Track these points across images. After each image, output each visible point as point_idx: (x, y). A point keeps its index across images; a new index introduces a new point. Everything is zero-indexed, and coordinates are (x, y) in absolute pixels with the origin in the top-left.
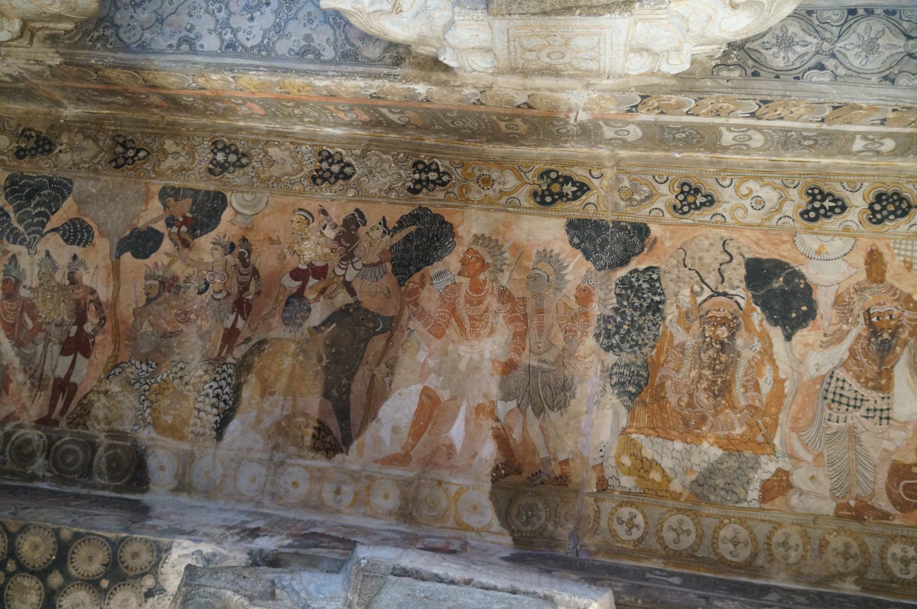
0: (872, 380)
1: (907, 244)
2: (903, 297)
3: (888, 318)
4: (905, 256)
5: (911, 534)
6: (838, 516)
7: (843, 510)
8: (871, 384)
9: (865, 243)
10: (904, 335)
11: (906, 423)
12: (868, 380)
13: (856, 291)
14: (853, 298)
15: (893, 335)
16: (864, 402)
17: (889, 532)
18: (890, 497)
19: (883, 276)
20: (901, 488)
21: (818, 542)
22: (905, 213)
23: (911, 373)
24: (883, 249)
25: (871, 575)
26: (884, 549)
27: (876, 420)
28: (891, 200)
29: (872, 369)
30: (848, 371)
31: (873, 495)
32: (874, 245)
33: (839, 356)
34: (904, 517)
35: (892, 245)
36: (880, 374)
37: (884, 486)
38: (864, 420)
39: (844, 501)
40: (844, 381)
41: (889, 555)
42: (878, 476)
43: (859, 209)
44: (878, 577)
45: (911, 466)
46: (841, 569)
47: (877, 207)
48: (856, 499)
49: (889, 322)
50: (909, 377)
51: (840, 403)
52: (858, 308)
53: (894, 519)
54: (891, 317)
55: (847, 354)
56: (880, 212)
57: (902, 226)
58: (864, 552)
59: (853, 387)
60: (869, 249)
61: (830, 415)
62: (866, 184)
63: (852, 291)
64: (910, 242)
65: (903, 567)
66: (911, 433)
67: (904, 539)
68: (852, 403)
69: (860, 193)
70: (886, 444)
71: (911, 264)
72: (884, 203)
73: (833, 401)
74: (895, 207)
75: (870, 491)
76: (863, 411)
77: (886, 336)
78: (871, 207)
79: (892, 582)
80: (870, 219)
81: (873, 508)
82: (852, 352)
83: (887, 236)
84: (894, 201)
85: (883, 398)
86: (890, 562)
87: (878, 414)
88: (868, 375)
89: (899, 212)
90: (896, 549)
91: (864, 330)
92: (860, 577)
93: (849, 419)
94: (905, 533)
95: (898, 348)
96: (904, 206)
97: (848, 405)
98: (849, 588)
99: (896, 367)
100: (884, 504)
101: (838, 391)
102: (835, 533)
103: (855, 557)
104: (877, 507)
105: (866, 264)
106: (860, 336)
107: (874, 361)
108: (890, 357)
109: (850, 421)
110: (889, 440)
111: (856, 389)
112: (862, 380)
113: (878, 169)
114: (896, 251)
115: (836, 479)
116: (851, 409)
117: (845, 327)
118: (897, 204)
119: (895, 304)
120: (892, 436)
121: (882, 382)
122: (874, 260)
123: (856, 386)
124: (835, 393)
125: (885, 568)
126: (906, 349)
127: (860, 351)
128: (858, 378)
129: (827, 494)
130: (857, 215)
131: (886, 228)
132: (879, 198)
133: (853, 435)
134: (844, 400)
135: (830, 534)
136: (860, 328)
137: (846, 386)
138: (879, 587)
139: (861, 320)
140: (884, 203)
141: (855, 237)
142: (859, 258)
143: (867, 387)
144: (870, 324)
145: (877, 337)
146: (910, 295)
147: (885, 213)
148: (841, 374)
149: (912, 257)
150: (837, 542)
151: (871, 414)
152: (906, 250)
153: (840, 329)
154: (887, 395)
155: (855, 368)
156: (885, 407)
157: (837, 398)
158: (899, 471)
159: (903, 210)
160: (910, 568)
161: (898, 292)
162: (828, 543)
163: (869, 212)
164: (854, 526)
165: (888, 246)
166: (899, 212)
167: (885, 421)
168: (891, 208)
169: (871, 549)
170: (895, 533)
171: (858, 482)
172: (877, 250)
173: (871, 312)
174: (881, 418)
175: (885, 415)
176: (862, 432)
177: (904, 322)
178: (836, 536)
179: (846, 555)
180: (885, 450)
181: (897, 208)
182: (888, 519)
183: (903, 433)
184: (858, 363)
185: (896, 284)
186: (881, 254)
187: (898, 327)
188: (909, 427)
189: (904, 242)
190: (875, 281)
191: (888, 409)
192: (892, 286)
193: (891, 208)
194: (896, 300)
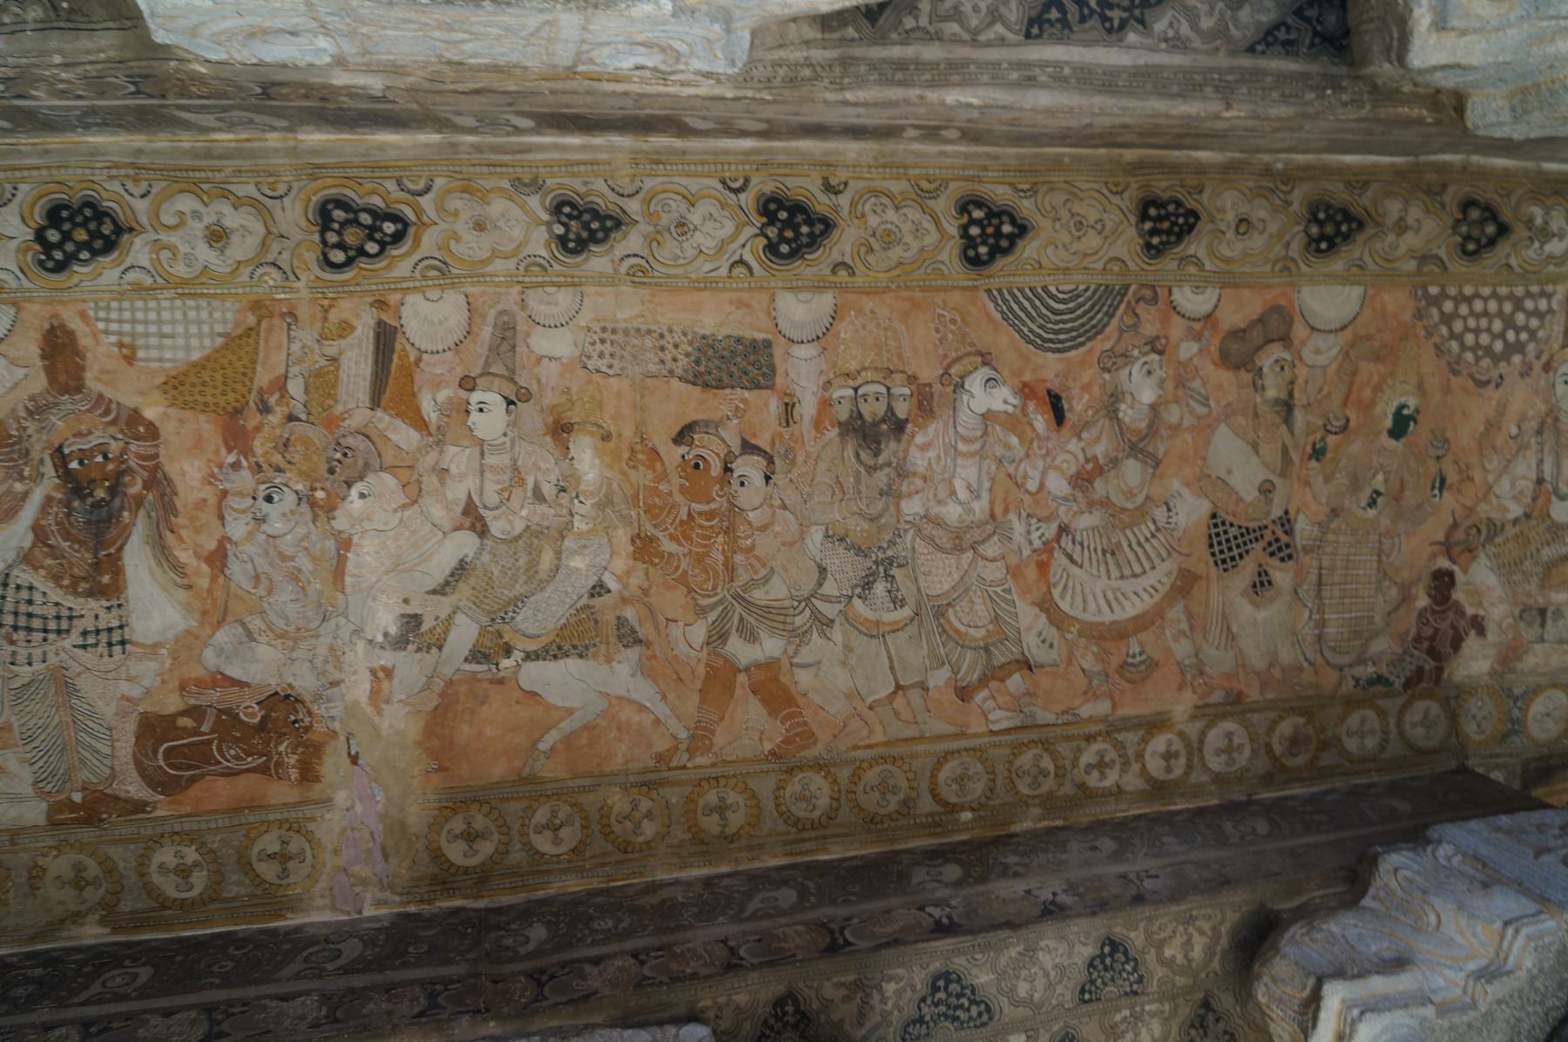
0: (84, 579)
1: (121, 309)
2: (124, 416)
3: (99, 459)
4: (120, 333)
5: (187, 827)
6: (54, 824)
7: (61, 812)
8: (83, 586)
9: (37, 315)
10: (135, 488)
11: (156, 646)
12: (76, 581)
13: (30, 413)
14: (25, 429)
15: (113, 491)
16: (75, 622)
17: (150, 832)
18: (143, 776)
19: (80, 379)
20: (160, 756)
21: (25, 873)
22: (110, 246)
23: (155, 556)
24: (75, 324)
25: (126, 906)
26: (143, 860)
27: (102, 648)
28: (79, 219)
29: (81, 558)
30: (36, 568)
31: (113, 776)
32: (56, 316)
33: (14, 543)
34: (171, 802)
35: (91, 313)
36: (97, 566)
37: (130, 758)
38: (80, 652)
39: (62, 797)
40: (31, 588)
41: (154, 867)
42: (117, 744)
43: (14, 243)
44: (139, 906)
45: (174, 717)
46: (73, 907)
47: (53, 236)
48: (84, 789)
49: (103, 465)
50: (153, 563)
51: (29, 629)
52: (38, 448)
53: (155, 808)
54: (105, 457)
55: (30, 537)
56: (59, 246)
57: (105, 273)
58: (110, 870)
59: (50, 595)
60: (47, 326)
61: (14, 653)
62: (24, 187)
63: (23, 414)
64: (126, 304)
65: (180, 880)
66: (168, 661)
67: (177, 838)
68: (52, 625)
69: (14, 207)
70: (124, 688)
71: (133, 348)
72: (66, 227)
73: (15, 628)
74: (89, 232)
75: (107, 771)
76: (74, 637)
77: (100, 493)
78: (40, 236)
79: (165, 908)
80: (41, 264)
81: (117, 798)
82: (38, 531)
83: (79, 296)
84: (87, 220)
85: (108, 608)
86: (156, 878)
87: (104, 637)
88: (76, 571)
89: (98, 244)
90: (165, 856)
91: (56, 488)
92: (109, 914)
93: (50, 655)
94: (177, 828)
95: (126, 514)
96: (107, 229)
97: (45, 631)
98: (92, 933)
99: (127, 548)
100: (134, 788)
101: (23, 608)
102: (54, 853)
103: (95, 883)
104: (123, 795)
105: (43, 357)
106: (48, 500)
107: (82, 543)
108: (113, 532)
109: (53, 660)
110: (129, 679)
111: (56, 599)
112: (66, 582)
113: (47, 152)
114: (101, 325)
115: (40, 763)
116: (51, 636)
117: (19, 487)
118: (92, 226)
119: (112, 430)
120: (133, 672)
121: (104, 579)
122: (59, 350)
123: (55, 595)
124: (16, 614)
125: (150, 889)
126: (142, 513)
127: (54, 528)
128: (56, 579)
129: (30, 791)
130: (12, 255)
131: (76, 279)
132: (54, 215)
133: (63, 683)
134: (37, 623)
135: (44, 856)
136: (48, 484)
137: (37, 597)
138: (141, 921)
139: (49, 470)
140: (66, 227)
141: (14, 304)
142: (29, 347)
143: (76, 594)
144: (65, 474)
145: (83, 499)
146: (136, 411)
147: (70, 247)
148: (23, 576)
149: (133, 335)
150: (58, 866)
151: (91, 640)
152: (120, 321)
153: (8, 492)
154: (115, 602)
155: (49, 562)
156: (115, 623)
157: (22, 621)
158: (153, 729)
159: (105, 238)
160: (191, 880)
161: (114, 406)
162: (44, 870)
163: (38, 247)
164: (86, 834)
165: (83, 315)
166: (98, 244)
167: (117, 649)
168: (81, 235)
169: (121, 865)
170: (159, 830)
171: (82, 761)
172: (62, 326)
173: (66, 451)
174: (110, 644)
175: (116, 637)
176: (79, 674)
177: (131, 463)
178: (56, 857)
179: (79, 882)
180: (123, 698)
181: (94, 235)
182: (144, 811)
183: (153, 665)
184: (54, 552)
185: (108, 393)
186: (71, 335)
187: (120, 474)
188: (164, 651)
189: (114, 304)
190: (66, 390)
191: (121, 627)
192: (101, 397)
193: (81, 235)
194: (114, 422)
